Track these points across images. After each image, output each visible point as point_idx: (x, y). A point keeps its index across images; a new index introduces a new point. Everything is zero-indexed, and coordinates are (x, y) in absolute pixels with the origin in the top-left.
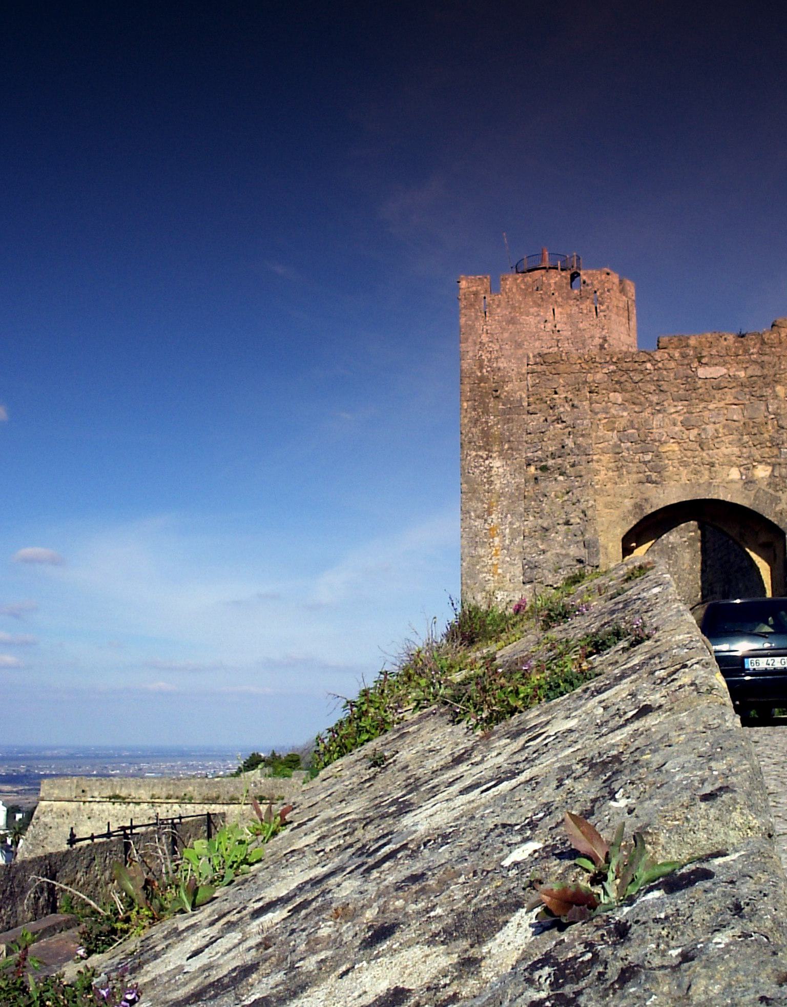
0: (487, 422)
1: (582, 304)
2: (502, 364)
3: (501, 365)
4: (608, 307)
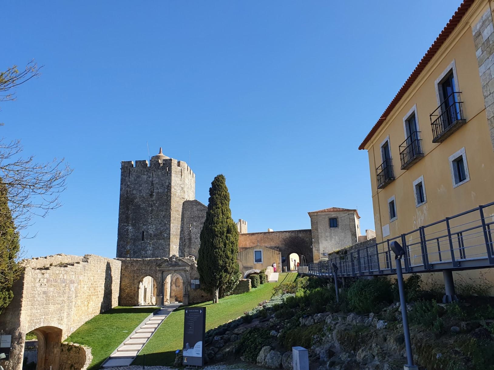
2: (134, 192)
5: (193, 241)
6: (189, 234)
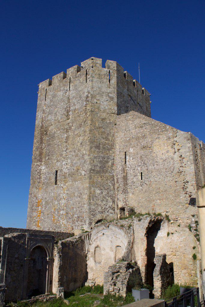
0: (42, 147)
1: (81, 78)
3: (49, 118)
4: (91, 75)
5: (129, 182)
6: (124, 170)
